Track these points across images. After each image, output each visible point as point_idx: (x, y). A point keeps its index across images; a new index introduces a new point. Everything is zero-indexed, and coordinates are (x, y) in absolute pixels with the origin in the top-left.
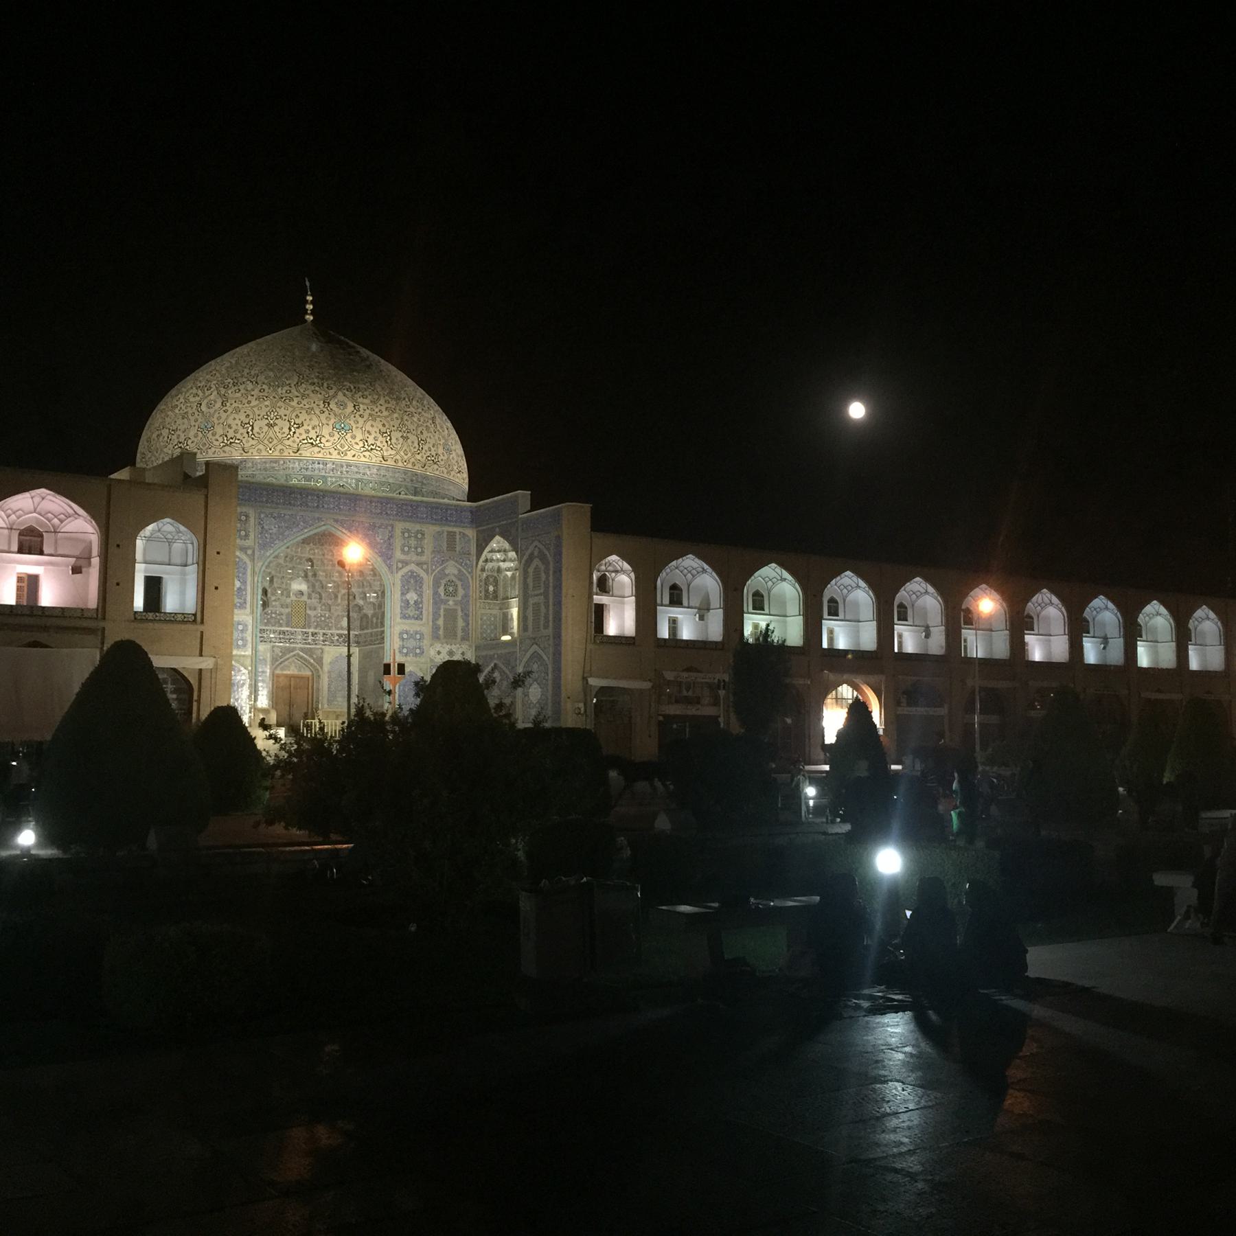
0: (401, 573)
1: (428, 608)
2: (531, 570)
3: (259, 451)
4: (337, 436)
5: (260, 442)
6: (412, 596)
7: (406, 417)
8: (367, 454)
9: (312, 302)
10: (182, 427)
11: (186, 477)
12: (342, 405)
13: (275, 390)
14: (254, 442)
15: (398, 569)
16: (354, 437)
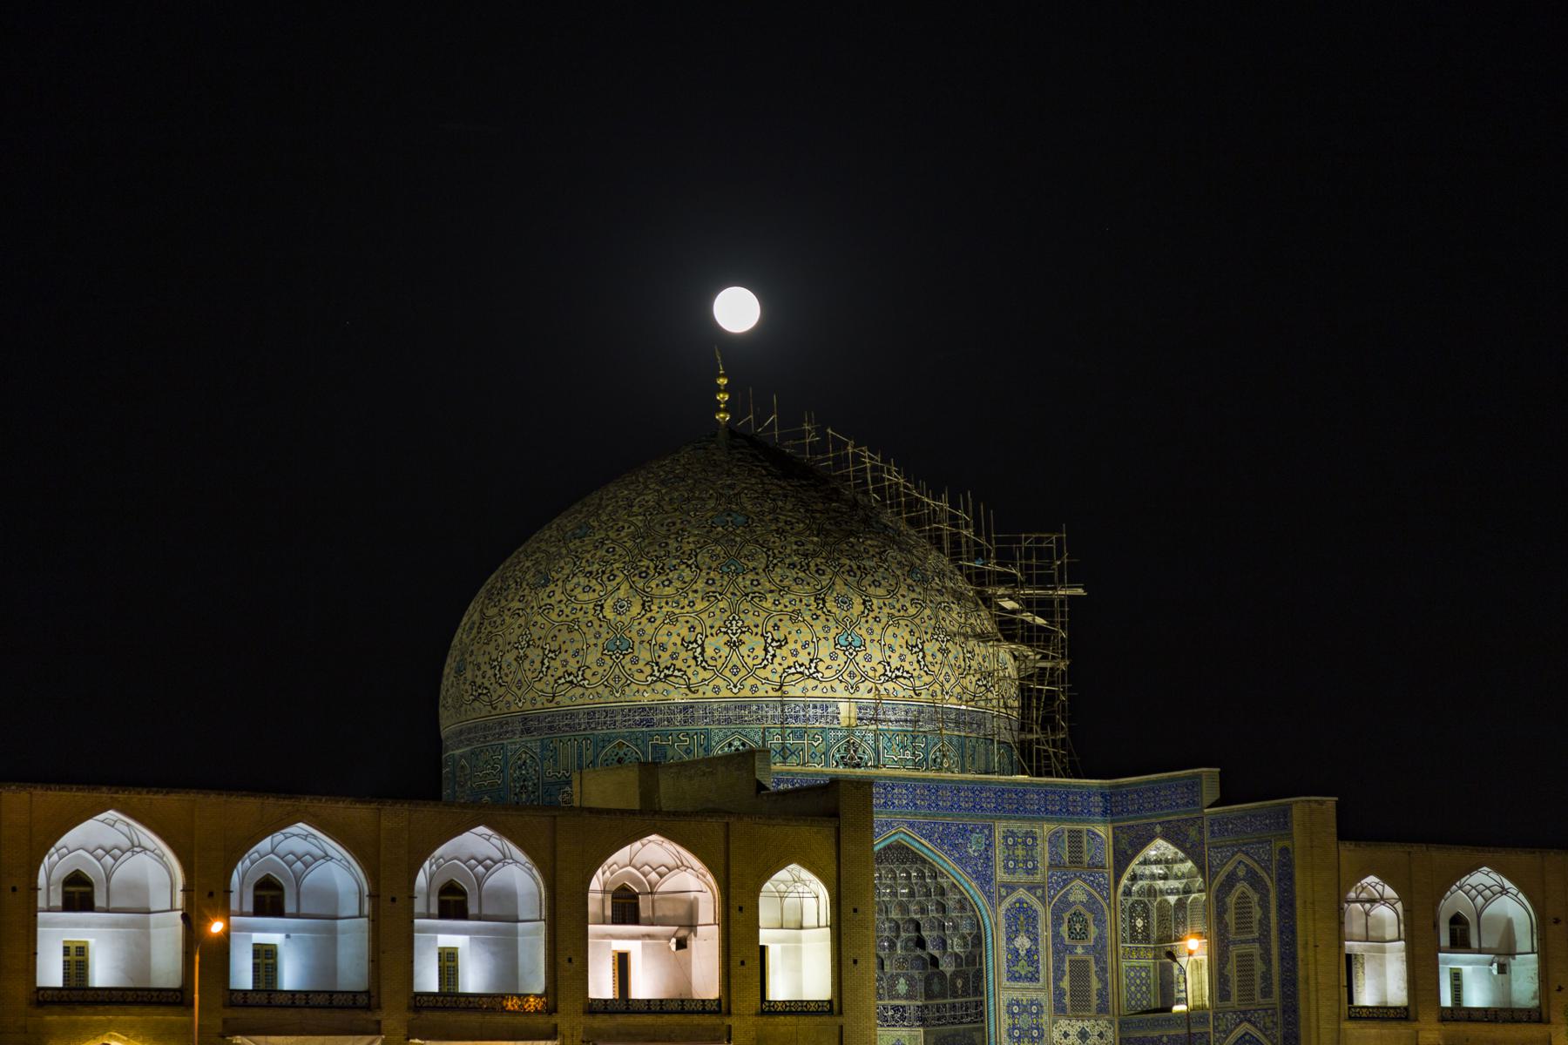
0: (1006, 904)
1: (1046, 959)
2: (1231, 900)
3: (717, 689)
4: (842, 659)
5: (718, 673)
6: (1023, 942)
7: (942, 614)
8: (890, 685)
9: (727, 389)
10: (572, 648)
11: (761, 787)
12: (845, 602)
13: (733, 582)
14: (707, 675)
15: (1002, 898)
16: (868, 658)
